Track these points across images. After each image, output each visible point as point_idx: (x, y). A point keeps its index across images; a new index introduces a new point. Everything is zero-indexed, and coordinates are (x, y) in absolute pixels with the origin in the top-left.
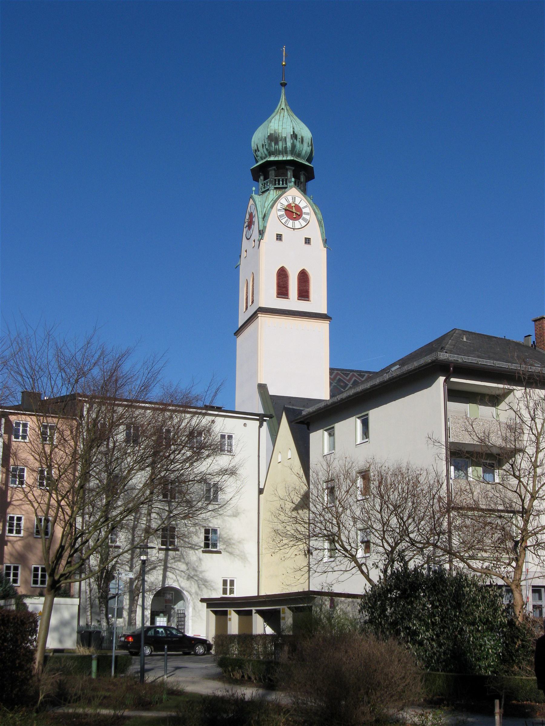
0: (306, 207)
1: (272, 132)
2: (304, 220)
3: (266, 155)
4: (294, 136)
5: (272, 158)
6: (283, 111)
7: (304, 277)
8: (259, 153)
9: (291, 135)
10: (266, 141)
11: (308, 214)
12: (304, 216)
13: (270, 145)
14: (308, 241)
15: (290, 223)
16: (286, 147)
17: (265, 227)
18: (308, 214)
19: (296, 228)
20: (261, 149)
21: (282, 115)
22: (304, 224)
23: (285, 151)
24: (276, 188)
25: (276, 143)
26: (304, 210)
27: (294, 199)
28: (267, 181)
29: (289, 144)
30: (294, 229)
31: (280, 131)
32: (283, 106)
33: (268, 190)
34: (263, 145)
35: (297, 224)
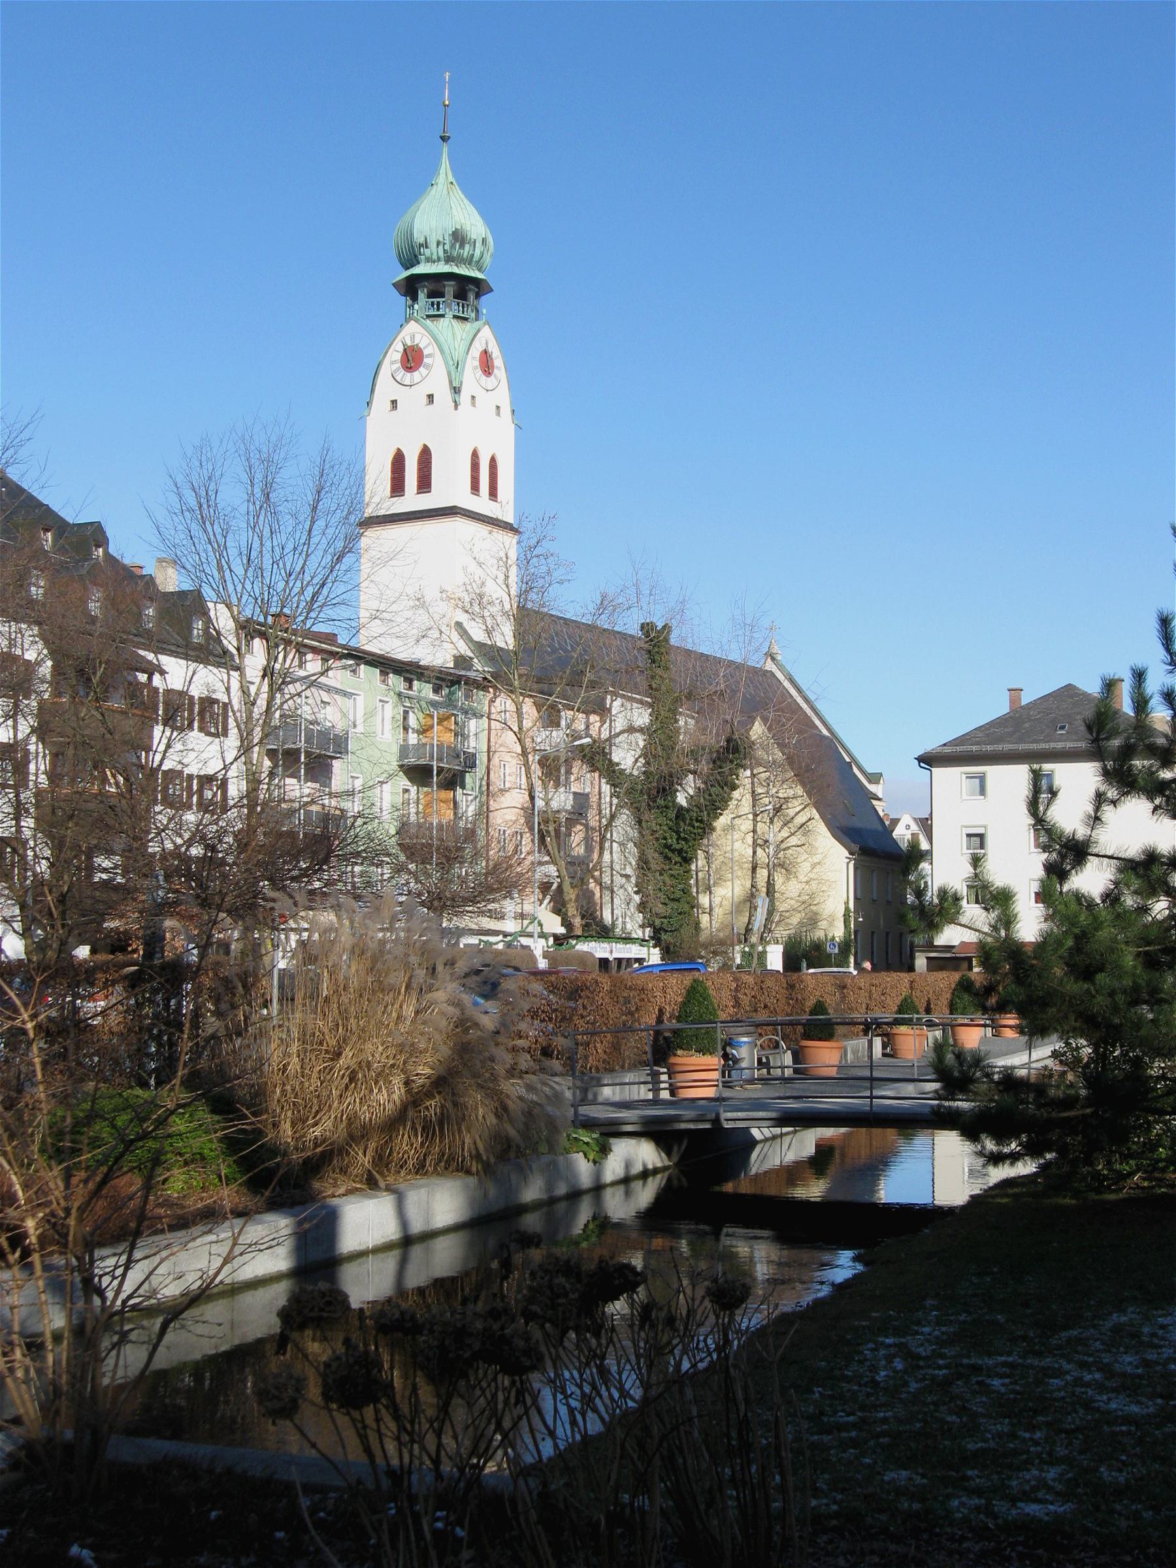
5: (456, 270)
7: (493, 461)
8: (427, 252)
10: (447, 237)
13: (453, 246)
16: (473, 255)
18: (499, 368)
20: (433, 245)
23: (469, 261)
24: (455, 317)
25: (462, 246)
28: (435, 300)
29: (477, 253)
32: (451, 178)
33: (442, 316)
34: (438, 243)
35: (490, 382)
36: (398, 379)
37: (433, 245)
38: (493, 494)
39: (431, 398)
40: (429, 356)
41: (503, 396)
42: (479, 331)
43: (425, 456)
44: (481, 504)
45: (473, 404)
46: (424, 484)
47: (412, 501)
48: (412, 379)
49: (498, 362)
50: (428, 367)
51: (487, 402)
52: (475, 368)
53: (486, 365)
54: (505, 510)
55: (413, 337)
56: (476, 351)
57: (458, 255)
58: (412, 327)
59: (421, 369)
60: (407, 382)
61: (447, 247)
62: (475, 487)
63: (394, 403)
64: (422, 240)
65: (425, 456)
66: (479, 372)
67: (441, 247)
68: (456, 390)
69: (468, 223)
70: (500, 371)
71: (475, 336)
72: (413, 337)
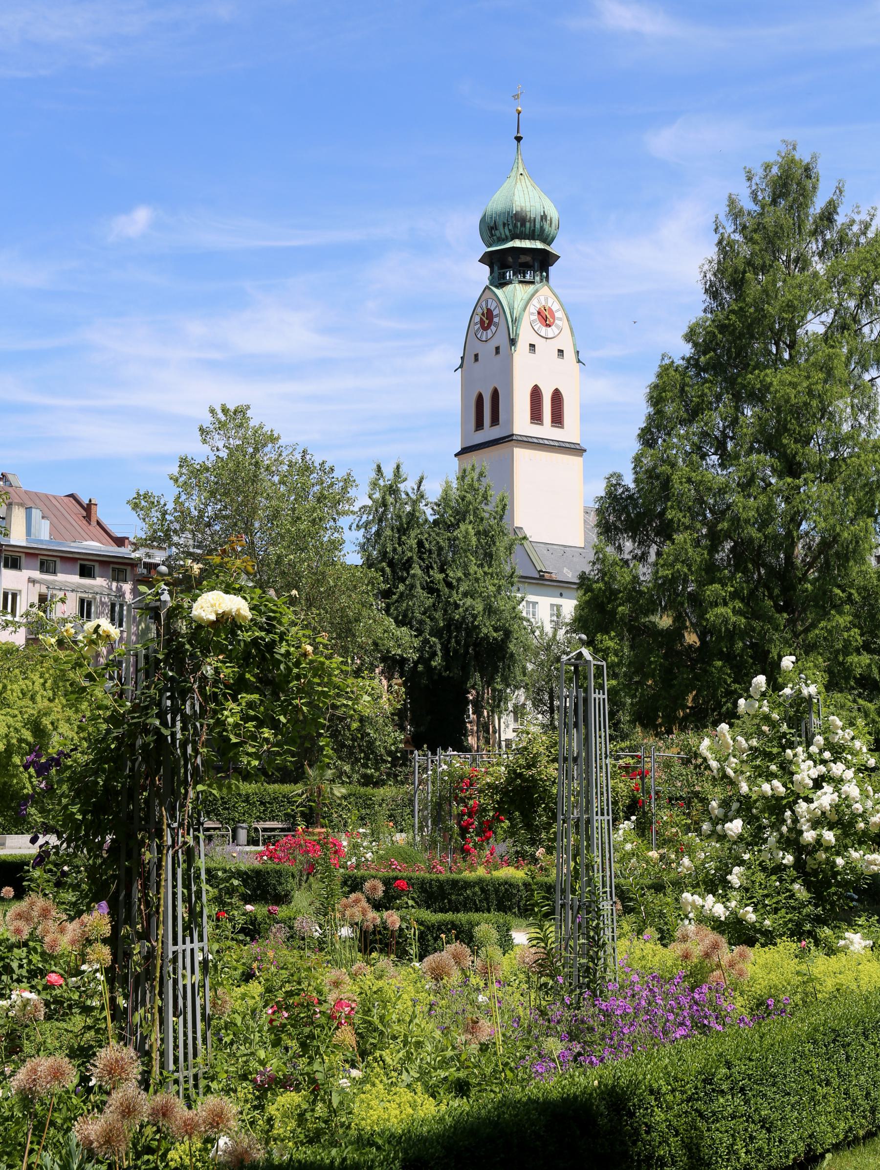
0: (558, 310)
1: (519, 209)
2: (557, 326)
3: (506, 236)
4: (544, 217)
5: (517, 243)
6: (522, 177)
7: (557, 397)
8: (497, 233)
9: (542, 217)
11: (560, 319)
12: (556, 321)
13: (515, 226)
14: (561, 352)
15: (543, 330)
16: (534, 230)
17: (517, 335)
18: (560, 319)
19: (549, 336)
21: (523, 184)
22: (557, 332)
25: (523, 224)
26: (557, 315)
27: (546, 300)
31: (528, 210)
34: (504, 225)
35: (550, 332)
37: (501, 227)
38: (558, 419)
39: (497, 349)
40: (497, 316)
42: (536, 291)
43: (495, 395)
44: (546, 431)
46: (495, 420)
47: (489, 433)
49: (559, 314)
50: (497, 325)
53: (545, 318)
54: (570, 433)
56: (533, 308)
57: (521, 232)
60: (484, 339)
61: (510, 227)
62: (536, 416)
63: (476, 357)
64: (492, 224)
65: (495, 395)
66: (538, 326)
67: (506, 228)
69: (528, 204)
71: (533, 295)
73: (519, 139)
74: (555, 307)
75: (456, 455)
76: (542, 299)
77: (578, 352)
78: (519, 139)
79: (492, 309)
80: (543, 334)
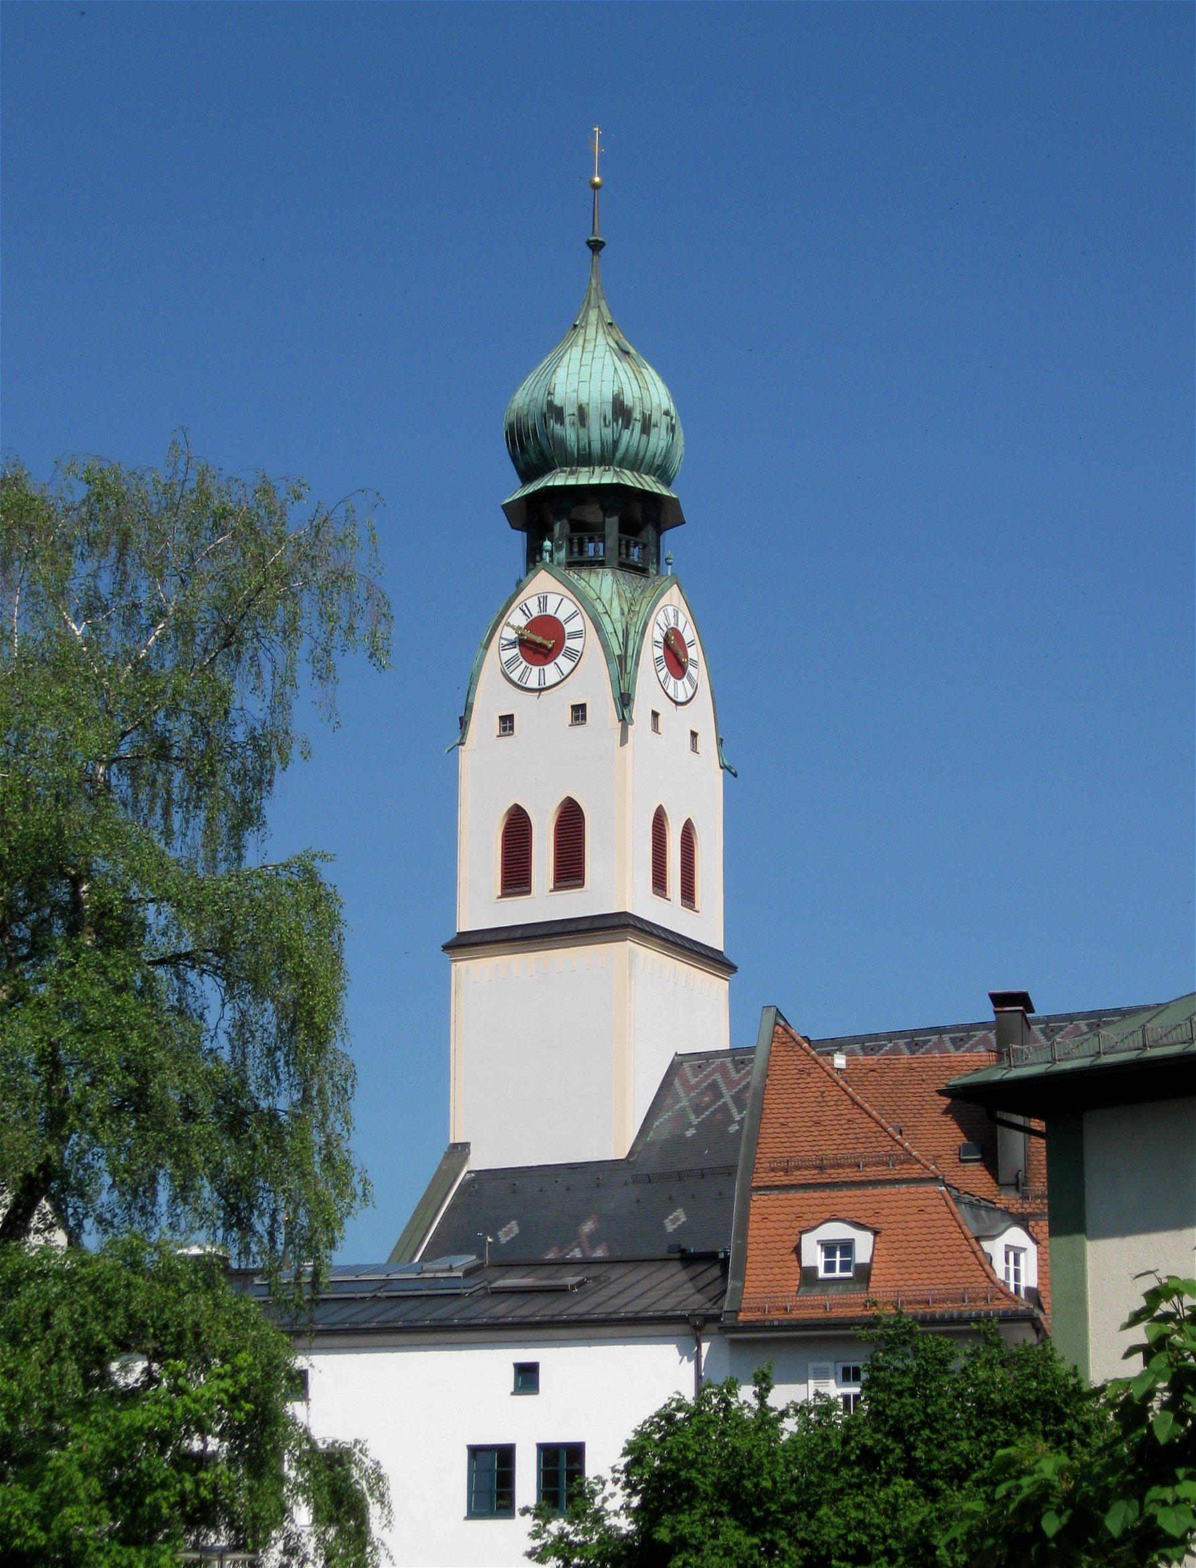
0: (692, 643)
18: (695, 664)
22: (690, 692)
27: (676, 616)
30: (677, 703)
35: (681, 689)
36: (515, 676)
39: (579, 712)
40: (577, 635)
41: (702, 715)
45: (655, 728)
48: (542, 674)
49: (694, 653)
51: (677, 723)
52: (658, 661)
55: (543, 602)
58: (543, 582)
59: (561, 660)
60: (533, 683)
63: (507, 722)
68: (624, 700)
70: (699, 672)
72: (543, 602)
73: (596, 246)
74: (689, 634)
75: (446, 947)
76: (670, 610)
77: (722, 740)
78: (596, 246)
79: (561, 616)
80: (671, 692)
